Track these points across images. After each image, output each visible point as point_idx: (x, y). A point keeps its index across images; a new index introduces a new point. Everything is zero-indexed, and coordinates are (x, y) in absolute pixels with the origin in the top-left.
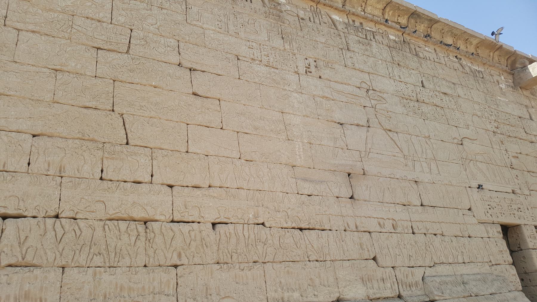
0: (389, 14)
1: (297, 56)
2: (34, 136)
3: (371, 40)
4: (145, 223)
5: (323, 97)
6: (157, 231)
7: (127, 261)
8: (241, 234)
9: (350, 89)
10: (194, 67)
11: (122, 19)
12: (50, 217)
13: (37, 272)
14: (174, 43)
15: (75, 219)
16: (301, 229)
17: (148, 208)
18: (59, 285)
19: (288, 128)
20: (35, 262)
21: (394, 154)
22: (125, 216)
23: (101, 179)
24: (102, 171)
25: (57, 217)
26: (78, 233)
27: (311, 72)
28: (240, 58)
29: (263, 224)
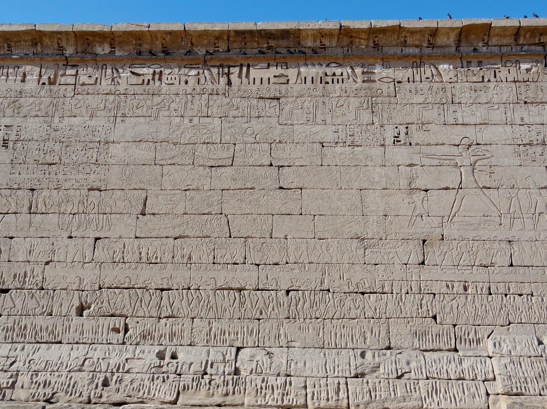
1: (386, 127)
2: (175, 239)
3: (489, 81)
4: (241, 291)
9: (445, 149)
10: (281, 164)
11: (228, 138)
12: (185, 289)
15: (199, 290)
16: (363, 293)
18: (190, 329)
23: (214, 263)
24: (214, 258)
26: (200, 298)
27: (400, 141)
28: (324, 144)
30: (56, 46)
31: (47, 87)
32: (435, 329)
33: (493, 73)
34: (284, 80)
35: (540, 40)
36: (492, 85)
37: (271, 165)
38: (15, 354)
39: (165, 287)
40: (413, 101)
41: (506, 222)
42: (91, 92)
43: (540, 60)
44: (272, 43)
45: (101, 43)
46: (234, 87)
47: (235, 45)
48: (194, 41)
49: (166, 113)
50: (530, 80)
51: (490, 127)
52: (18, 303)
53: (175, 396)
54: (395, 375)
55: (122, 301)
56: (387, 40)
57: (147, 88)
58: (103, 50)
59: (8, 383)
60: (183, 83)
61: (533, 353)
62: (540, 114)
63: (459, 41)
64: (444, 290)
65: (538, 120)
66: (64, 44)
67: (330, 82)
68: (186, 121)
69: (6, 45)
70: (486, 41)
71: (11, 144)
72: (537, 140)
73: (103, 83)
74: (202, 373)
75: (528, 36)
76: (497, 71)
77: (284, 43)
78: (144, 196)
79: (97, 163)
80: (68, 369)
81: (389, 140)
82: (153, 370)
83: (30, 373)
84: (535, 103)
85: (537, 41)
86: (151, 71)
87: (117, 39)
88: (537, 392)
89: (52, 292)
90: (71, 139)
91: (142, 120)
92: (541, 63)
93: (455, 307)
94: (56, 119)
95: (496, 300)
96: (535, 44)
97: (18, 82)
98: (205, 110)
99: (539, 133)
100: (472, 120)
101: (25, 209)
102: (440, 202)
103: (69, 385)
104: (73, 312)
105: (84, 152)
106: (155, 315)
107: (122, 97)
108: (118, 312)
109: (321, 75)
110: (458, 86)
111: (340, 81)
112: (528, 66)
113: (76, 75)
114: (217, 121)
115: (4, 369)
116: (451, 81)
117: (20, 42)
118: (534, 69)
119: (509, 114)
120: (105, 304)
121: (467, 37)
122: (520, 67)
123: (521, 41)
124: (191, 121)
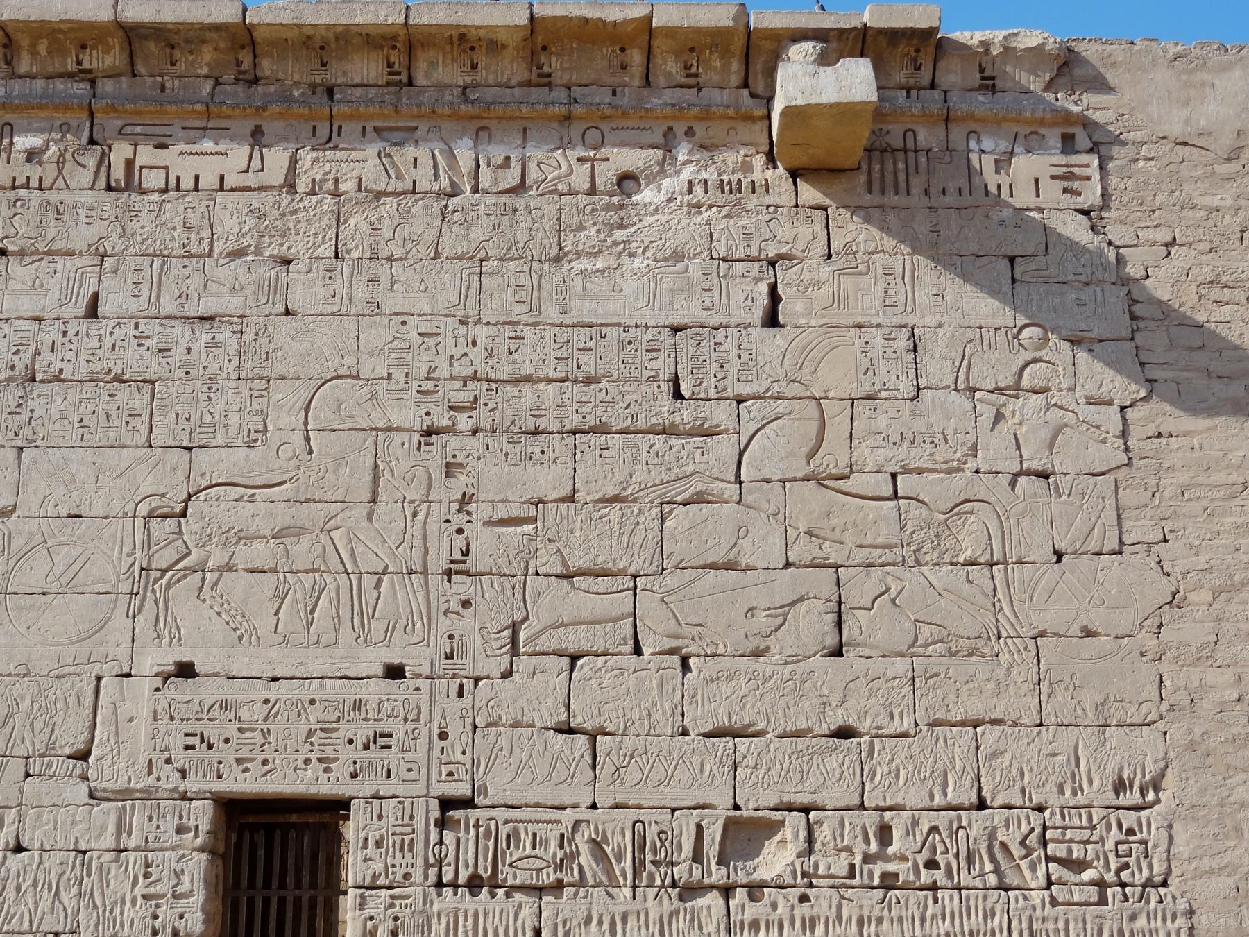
35: (79, 63)
43: (74, 123)
50: (34, 183)
62: (37, 285)
65: (28, 306)
72: (13, 367)
75: (42, 48)
84: (32, 254)
85: (71, 66)
92: (77, 135)
96: (71, 76)
112: (35, 141)
118: (53, 149)
122: (11, 144)
123: (24, 65)
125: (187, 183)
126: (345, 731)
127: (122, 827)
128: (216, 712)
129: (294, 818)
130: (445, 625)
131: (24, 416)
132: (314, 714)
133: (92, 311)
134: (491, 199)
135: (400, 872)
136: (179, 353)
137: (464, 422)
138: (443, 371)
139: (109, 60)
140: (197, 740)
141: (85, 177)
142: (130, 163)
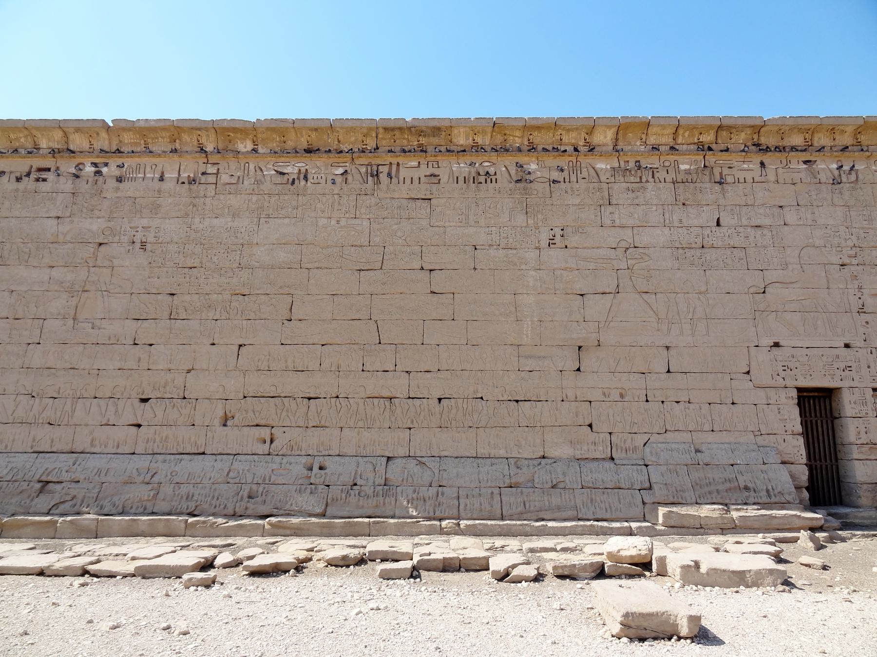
0: (683, 136)
5: (565, 269)
6: (397, 405)
7: (378, 424)
8: (460, 406)
9: (602, 252)
10: (432, 268)
11: (377, 239)
13: (327, 430)
14: (417, 249)
17: (392, 389)
19: (518, 309)
20: (326, 425)
21: (644, 319)
22: (377, 395)
25: (337, 397)
29: (482, 398)
30: (196, 143)
31: (186, 186)
32: (592, 437)
33: (651, 173)
34: (435, 180)
36: (649, 186)
37: (422, 268)
38: (156, 465)
39: (312, 396)
40: (570, 203)
41: (664, 327)
42: (232, 191)
44: (423, 140)
45: (243, 140)
46: (383, 186)
47: (384, 142)
48: (341, 138)
49: (313, 214)
51: (648, 229)
52: (160, 413)
53: (323, 508)
54: (550, 485)
55: (268, 411)
56: (542, 138)
57: (292, 188)
58: (245, 147)
59: (149, 496)
60: (329, 182)
61: (690, 462)
63: (617, 140)
64: (602, 398)
65: (696, 222)
66: (203, 140)
67: (483, 181)
68: (333, 222)
69: (142, 142)
70: (644, 140)
71: (149, 247)
73: (245, 182)
74: (351, 483)
75: (686, 134)
76: (655, 171)
77: (435, 140)
78: (289, 300)
79: (240, 267)
80: (212, 481)
81: (544, 243)
82: (300, 481)
83: (172, 485)
85: (696, 141)
86: (296, 171)
87: (259, 136)
88: (694, 500)
89: (194, 401)
90: (213, 242)
91: (287, 221)
93: (611, 414)
94: (197, 220)
95: (654, 406)
97: (156, 180)
98: (353, 210)
99: (697, 236)
100: (631, 222)
101: (166, 315)
102: (596, 307)
103: (213, 497)
104: (217, 422)
105: (226, 254)
106: (301, 424)
107: (266, 197)
108: (263, 422)
109: (473, 174)
110: (616, 186)
111: (494, 180)
113: (217, 174)
114: (366, 223)
115: (147, 480)
116: (608, 181)
117: (157, 138)
119: (667, 216)
120: (251, 414)
121: (625, 135)
124: (338, 222)
125: (742, 180)
126: (836, 366)
127: (768, 398)
128: (791, 359)
129: (805, 394)
130: (862, 330)
131: (703, 259)
132: (824, 359)
133: (718, 224)
134: (848, 185)
135: (864, 412)
136: (751, 239)
137: (854, 261)
138: (843, 244)
139: (709, 138)
140: (786, 368)
141: (707, 178)
142: (721, 174)
